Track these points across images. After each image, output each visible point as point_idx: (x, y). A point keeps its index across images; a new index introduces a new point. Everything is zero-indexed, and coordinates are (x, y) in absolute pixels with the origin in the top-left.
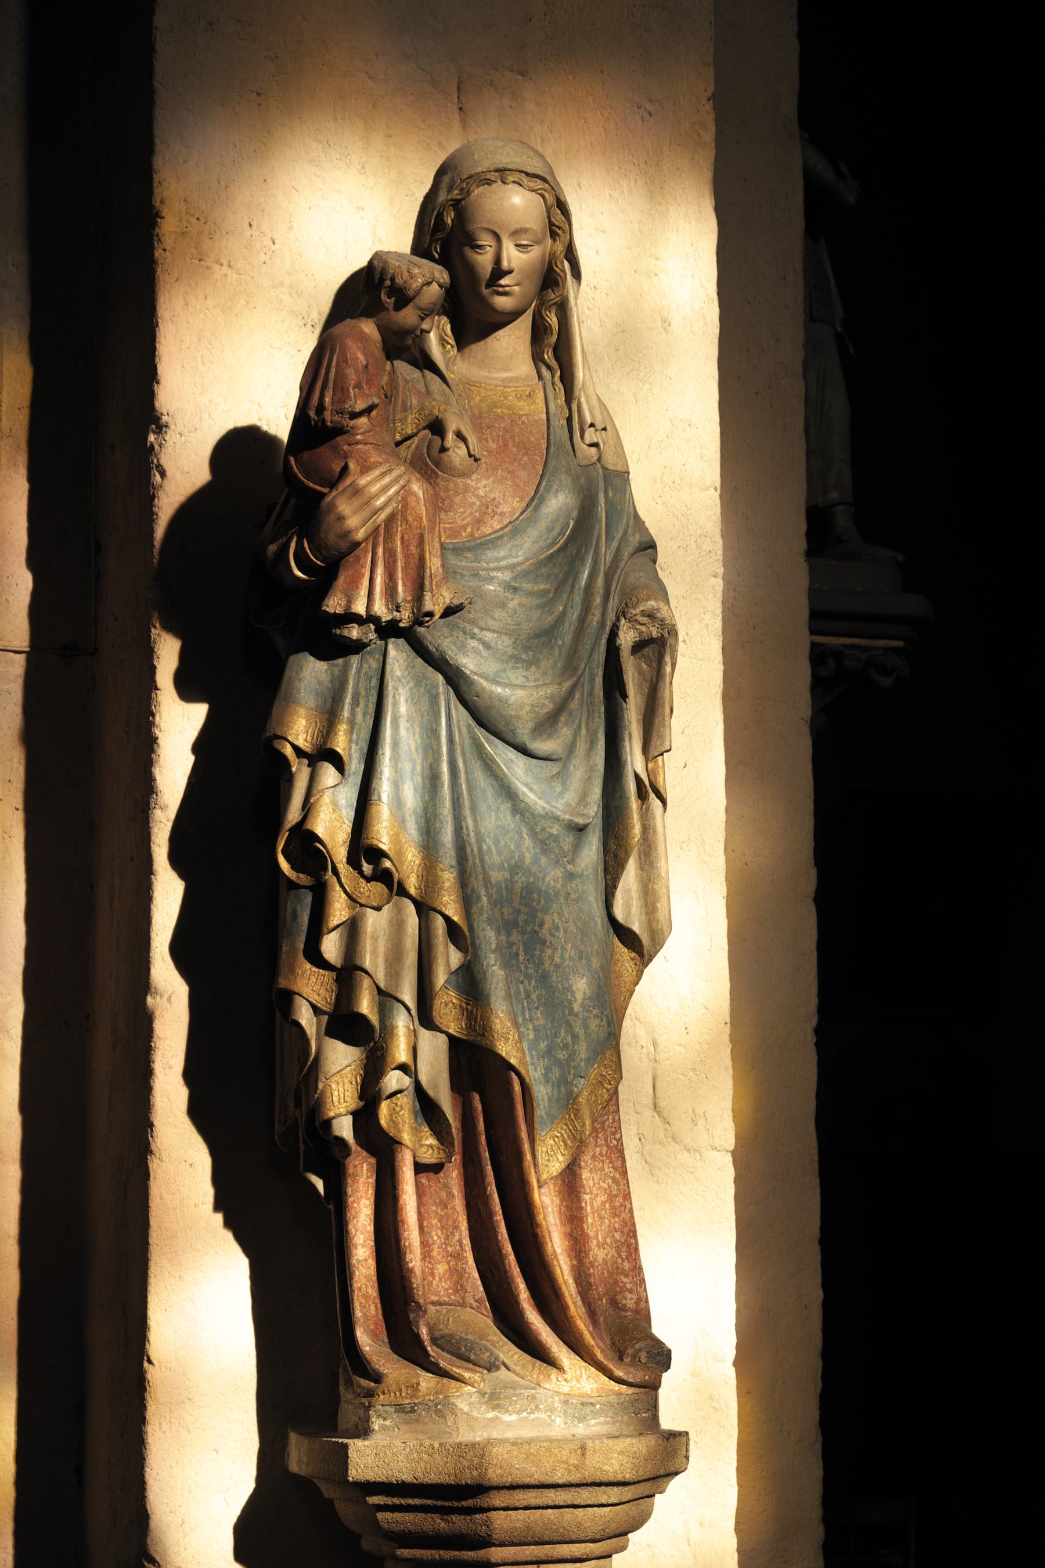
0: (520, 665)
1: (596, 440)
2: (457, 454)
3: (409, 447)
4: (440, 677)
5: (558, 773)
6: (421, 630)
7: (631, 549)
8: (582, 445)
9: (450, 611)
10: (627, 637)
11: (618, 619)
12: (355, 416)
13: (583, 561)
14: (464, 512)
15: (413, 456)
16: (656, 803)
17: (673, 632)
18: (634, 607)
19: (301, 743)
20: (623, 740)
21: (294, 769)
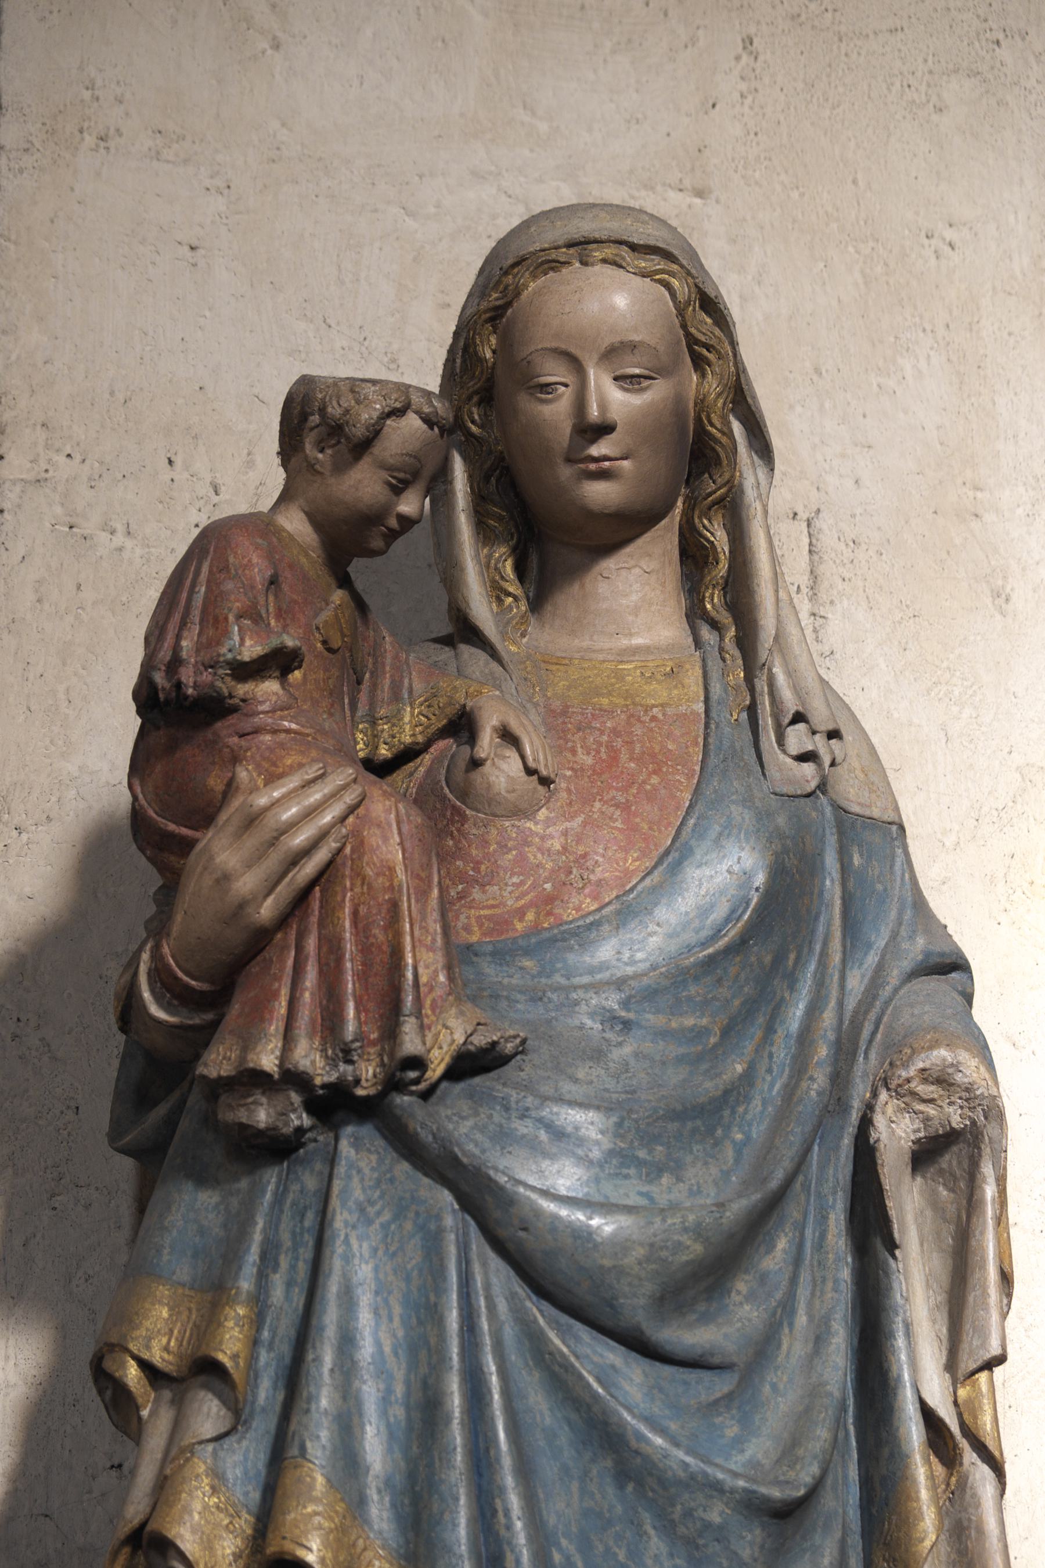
0: (632, 1171)
1: (810, 747)
2: (504, 772)
3: (411, 774)
4: (446, 1197)
5: (729, 1397)
6: (402, 1100)
7: (906, 965)
8: (782, 756)
9: (473, 1064)
10: (896, 1131)
11: (875, 1095)
12: (246, 671)
13: (792, 981)
14: (522, 883)
15: (421, 787)
16: (981, 1474)
17: (995, 1112)
18: (906, 1065)
19: (157, 1356)
20: (892, 1335)
21: (145, 1413)
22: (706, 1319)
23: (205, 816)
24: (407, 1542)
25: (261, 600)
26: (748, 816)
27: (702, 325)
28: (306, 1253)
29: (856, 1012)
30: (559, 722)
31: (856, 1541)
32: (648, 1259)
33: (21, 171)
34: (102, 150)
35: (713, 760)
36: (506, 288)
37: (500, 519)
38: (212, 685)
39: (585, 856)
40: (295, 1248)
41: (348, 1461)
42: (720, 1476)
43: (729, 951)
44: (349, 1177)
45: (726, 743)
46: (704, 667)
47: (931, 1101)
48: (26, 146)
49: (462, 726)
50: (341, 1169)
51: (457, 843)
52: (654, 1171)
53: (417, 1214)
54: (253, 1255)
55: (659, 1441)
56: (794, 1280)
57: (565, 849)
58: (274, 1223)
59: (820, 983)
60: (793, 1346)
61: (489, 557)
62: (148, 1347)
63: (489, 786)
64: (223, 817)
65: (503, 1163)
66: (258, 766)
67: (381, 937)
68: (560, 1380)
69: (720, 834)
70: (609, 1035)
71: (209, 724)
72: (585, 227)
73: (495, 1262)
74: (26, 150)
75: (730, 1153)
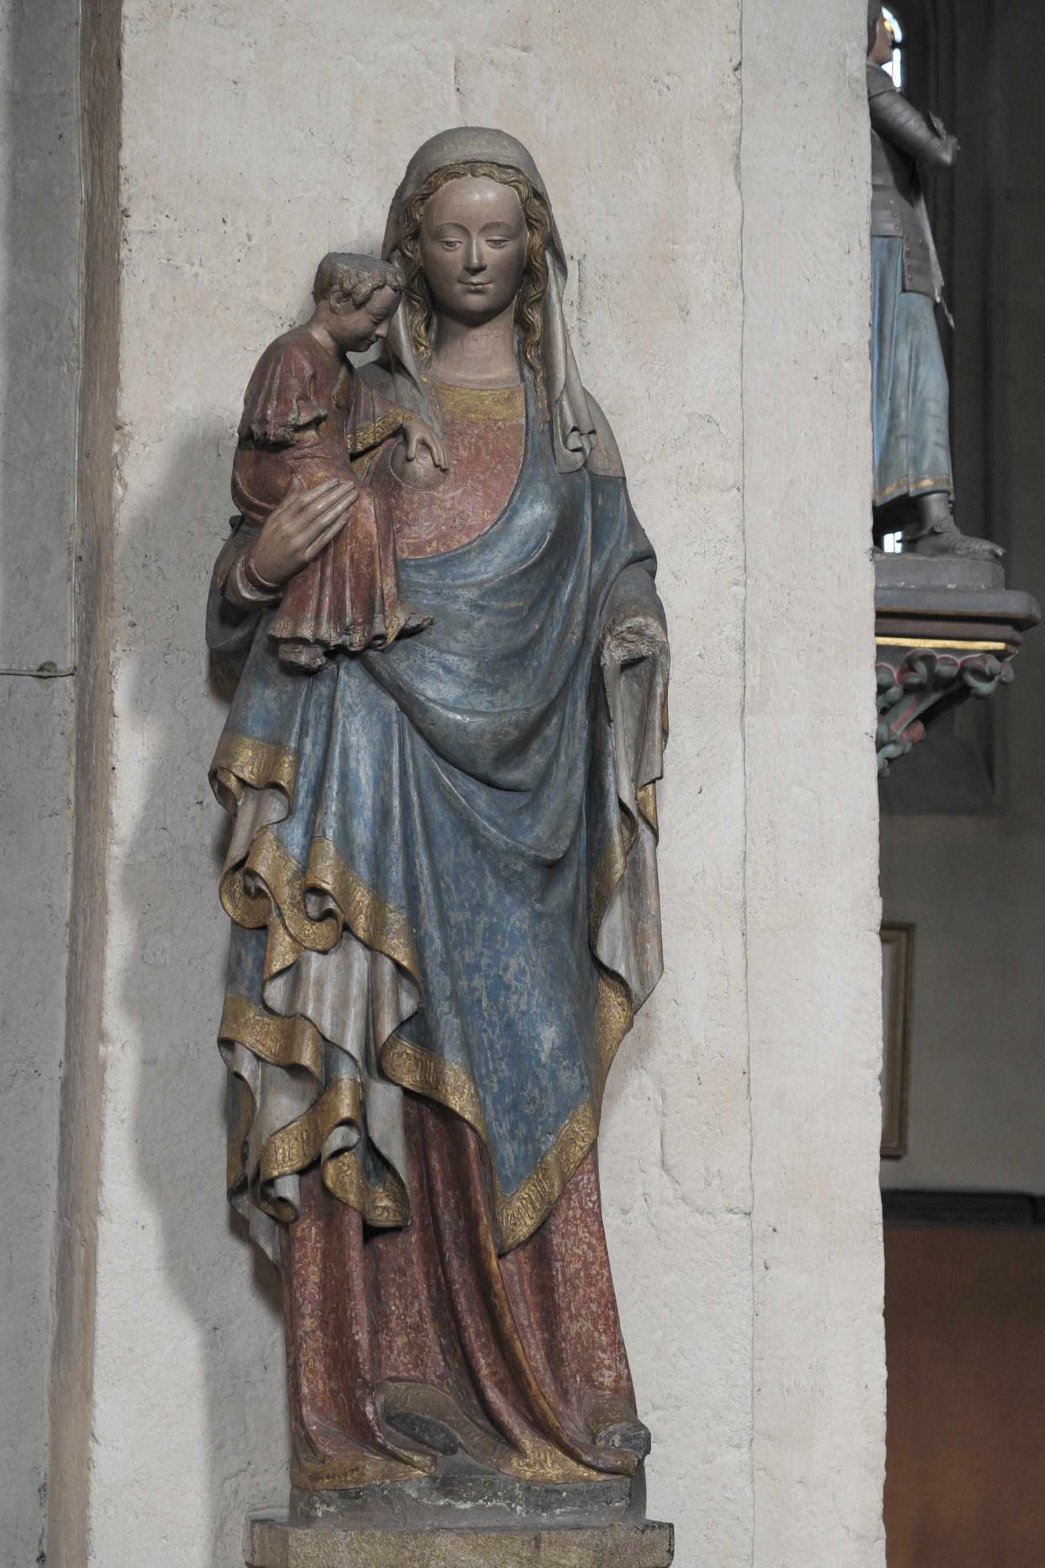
0: (484, 690)
1: (580, 445)
2: (422, 465)
3: (372, 458)
4: (393, 704)
5: (527, 805)
6: (372, 653)
7: (623, 560)
8: (565, 450)
9: (405, 634)
10: (614, 655)
11: (604, 638)
12: (298, 428)
13: (565, 576)
14: (430, 526)
15: (377, 466)
16: (646, 834)
17: (665, 650)
18: (621, 624)
19: (246, 775)
20: (606, 767)
21: (239, 803)
22: (517, 765)
23: (277, 498)
24: (373, 879)
25: (307, 386)
26: (547, 488)
27: (533, 210)
28: (323, 728)
29: (596, 588)
30: (451, 431)
31: (584, 869)
32: (492, 740)
33: (138, 33)
34: (183, 19)
35: (529, 456)
36: (430, 183)
37: (418, 302)
38: (283, 437)
39: (462, 512)
40: (317, 724)
41: (345, 838)
42: (523, 849)
43: (535, 565)
44: (345, 690)
45: (537, 444)
46: (526, 395)
47: (633, 642)
48: (141, 17)
49: (401, 433)
50: (341, 687)
51: (397, 501)
52: (493, 689)
53: (379, 712)
54: (296, 730)
55: (494, 831)
56: (559, 739)
57: (453, 508)
58: (305, 712)
59: (579, 577)
60: (560, 774)
61: (412, 322)
62: (243, 772)
63: (415, 473)
64: (286, 503)
65: (421, 687)
66: (304, 476)
67: (365, 570)
68: (446, 797)
69: (532, 500)
70: (474, 614)
71: (279, 451)
72: (475, 150)
73: (418, 738)
74: (141, 20)
75: (531, 674)
